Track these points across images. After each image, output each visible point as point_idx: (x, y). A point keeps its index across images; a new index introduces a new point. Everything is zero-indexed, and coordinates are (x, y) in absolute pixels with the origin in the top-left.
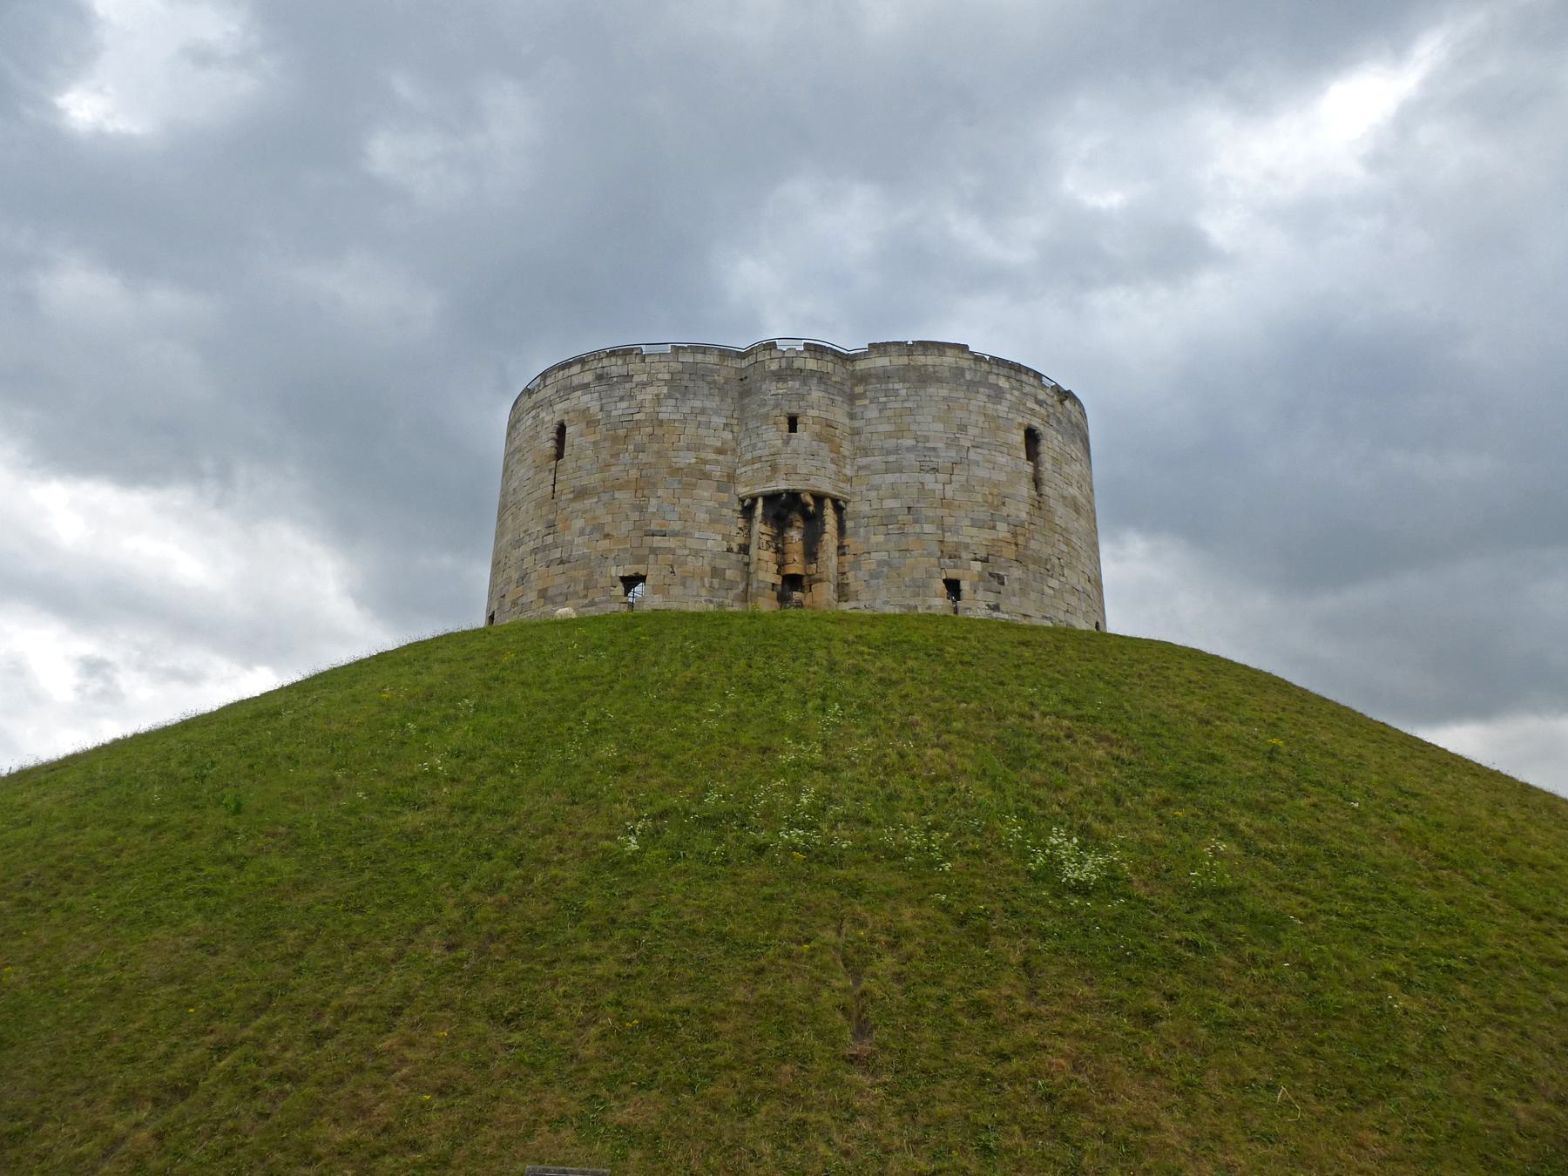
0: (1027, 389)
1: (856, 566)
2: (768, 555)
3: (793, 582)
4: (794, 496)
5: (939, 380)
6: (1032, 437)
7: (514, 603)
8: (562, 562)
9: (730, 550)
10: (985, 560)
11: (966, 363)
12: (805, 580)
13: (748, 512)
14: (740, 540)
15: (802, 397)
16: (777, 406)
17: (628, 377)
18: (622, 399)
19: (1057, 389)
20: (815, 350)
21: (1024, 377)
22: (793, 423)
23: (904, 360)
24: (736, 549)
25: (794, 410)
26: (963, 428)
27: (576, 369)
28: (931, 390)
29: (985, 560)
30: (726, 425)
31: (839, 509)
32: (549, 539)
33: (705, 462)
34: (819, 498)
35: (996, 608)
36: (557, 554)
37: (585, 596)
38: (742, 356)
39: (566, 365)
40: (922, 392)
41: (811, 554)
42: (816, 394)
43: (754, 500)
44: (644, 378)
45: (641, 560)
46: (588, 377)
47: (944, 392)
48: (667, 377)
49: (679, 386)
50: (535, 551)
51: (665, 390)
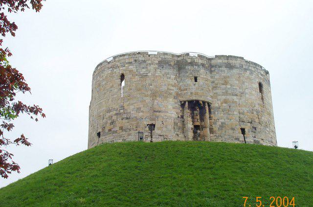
1: (215, 123)
2: (190, 119)
3: (197, 127)
4: (197, 101)
5: (237, 68)
6: (260, 85)
7: (110, 130)
8: (127, 118)
9: (178, 117)
11: (244, 63)
12: (200, 127)
13: (183, 105)
14: (181, 114)
15: (198, 71)
16: (191, 73)
17: (144, 61)
18: (143, 68)
19: (265, 70)
20: (201, 57)
21: (258, 68)
23: (226, 61)
25: (196, 75)
27: (126, 57)
29: (251, 123)
31: (209, 106)
32: (122, 111)
33: (170, 90)
34: (204, 102)
35: (255, 137)
36: (125, 116)
37: (137, 130)
38: (178, 56)
39: (124, 55)
40: (231, 71)
41: (202, 119)
42: (202, 71)
43: (185, 102)
44: (150, 62)
45: (154, 120)
46: (132, 60)
50: (117, 114)
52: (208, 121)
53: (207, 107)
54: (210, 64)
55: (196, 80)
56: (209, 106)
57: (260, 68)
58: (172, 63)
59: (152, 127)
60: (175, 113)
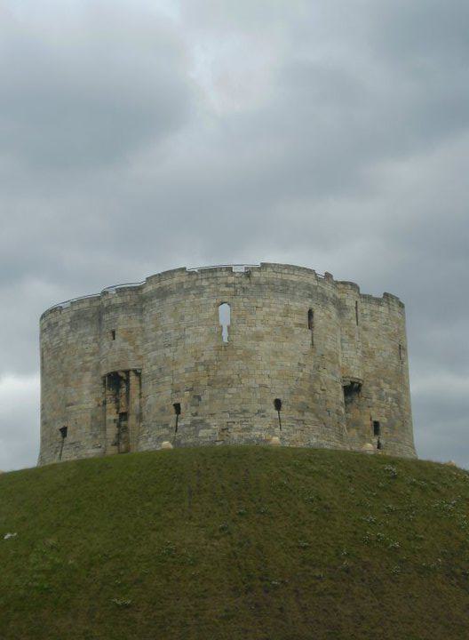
0: (221, 280)
5: (172, 293)
9: (99, 405)
10: (191, 390)
15: (115, 320)
20: (121, 291)
21: (218, 274)
22: (113, 333)
24: (101, 404)
26: (182, 318)
29: (191, 390)
31: (138, 374)
33: (87, 362)
34: (127, 372)
35: (196, 414)
47: (173, 300)
48: (69, 320)
51: (69, 327)
52: (136, 402)
53: (133, 378)
54: (136, 298)
55: (114, 339)
56: (138, 374)
59: (64, 431)
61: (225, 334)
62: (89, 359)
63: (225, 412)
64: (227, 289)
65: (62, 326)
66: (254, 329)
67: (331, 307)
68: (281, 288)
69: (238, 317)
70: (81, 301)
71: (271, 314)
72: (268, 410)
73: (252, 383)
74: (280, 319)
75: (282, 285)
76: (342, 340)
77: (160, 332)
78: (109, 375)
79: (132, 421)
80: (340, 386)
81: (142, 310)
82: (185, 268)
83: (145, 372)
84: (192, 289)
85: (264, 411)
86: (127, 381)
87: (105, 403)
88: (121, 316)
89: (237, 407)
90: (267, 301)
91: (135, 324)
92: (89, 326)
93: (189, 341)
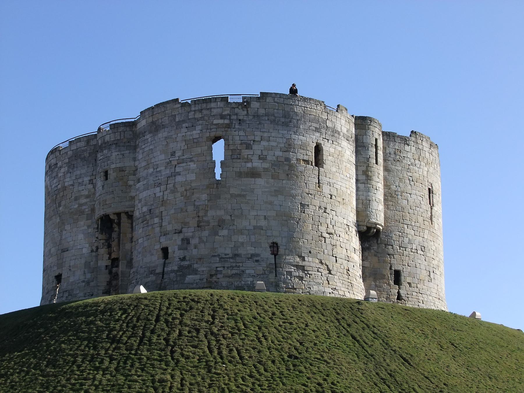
0: (215, 112)
5: (164, 127)
9: (92, 251)
14: (96, 244)
15: (108, 158)
20: (115, 127)
21: (213, 105)
22: (106, 173)
24: (94, 249)
26: (173, 154)
28: (160, 135)
29: (180, 232)
30: (90, 180)
33: (81, 205)
34: (118, 215)
42: (115, 154)
47: (165, 134)
49: (71, 166)
55: (107, 179)
56: (130, 216)
57: (220, 104)
58: (86, 155)
60: (87, 245)
61: (218, 171)
62: (83, 201)
63: (214, 256)
64: (221, 121)
65: (61, 167)
66: (249, 165)
67: (344, 143)
68: (283, 120)
69: (232, 154)
70: (78, 140)
71: (271, 149)
72: (262, 256)
73: (245, 223)
74: (281, 154)
75: (285, 117)
76: (357, 180)
77: (151, 170)
78: (101, 218)
79: (122, 267)
80: (353, 230)
81: (135, 148)
82: (177, 99)
83: (137, 214)
84: (184, 121)
85: (258, 255)
86: (119, 224)
87: (97, 248)
88: (115, 154)
89: (228, 251)
90: (266, 135)
91: (128, 163)
92: (86, 167)
93: (179, 179)
